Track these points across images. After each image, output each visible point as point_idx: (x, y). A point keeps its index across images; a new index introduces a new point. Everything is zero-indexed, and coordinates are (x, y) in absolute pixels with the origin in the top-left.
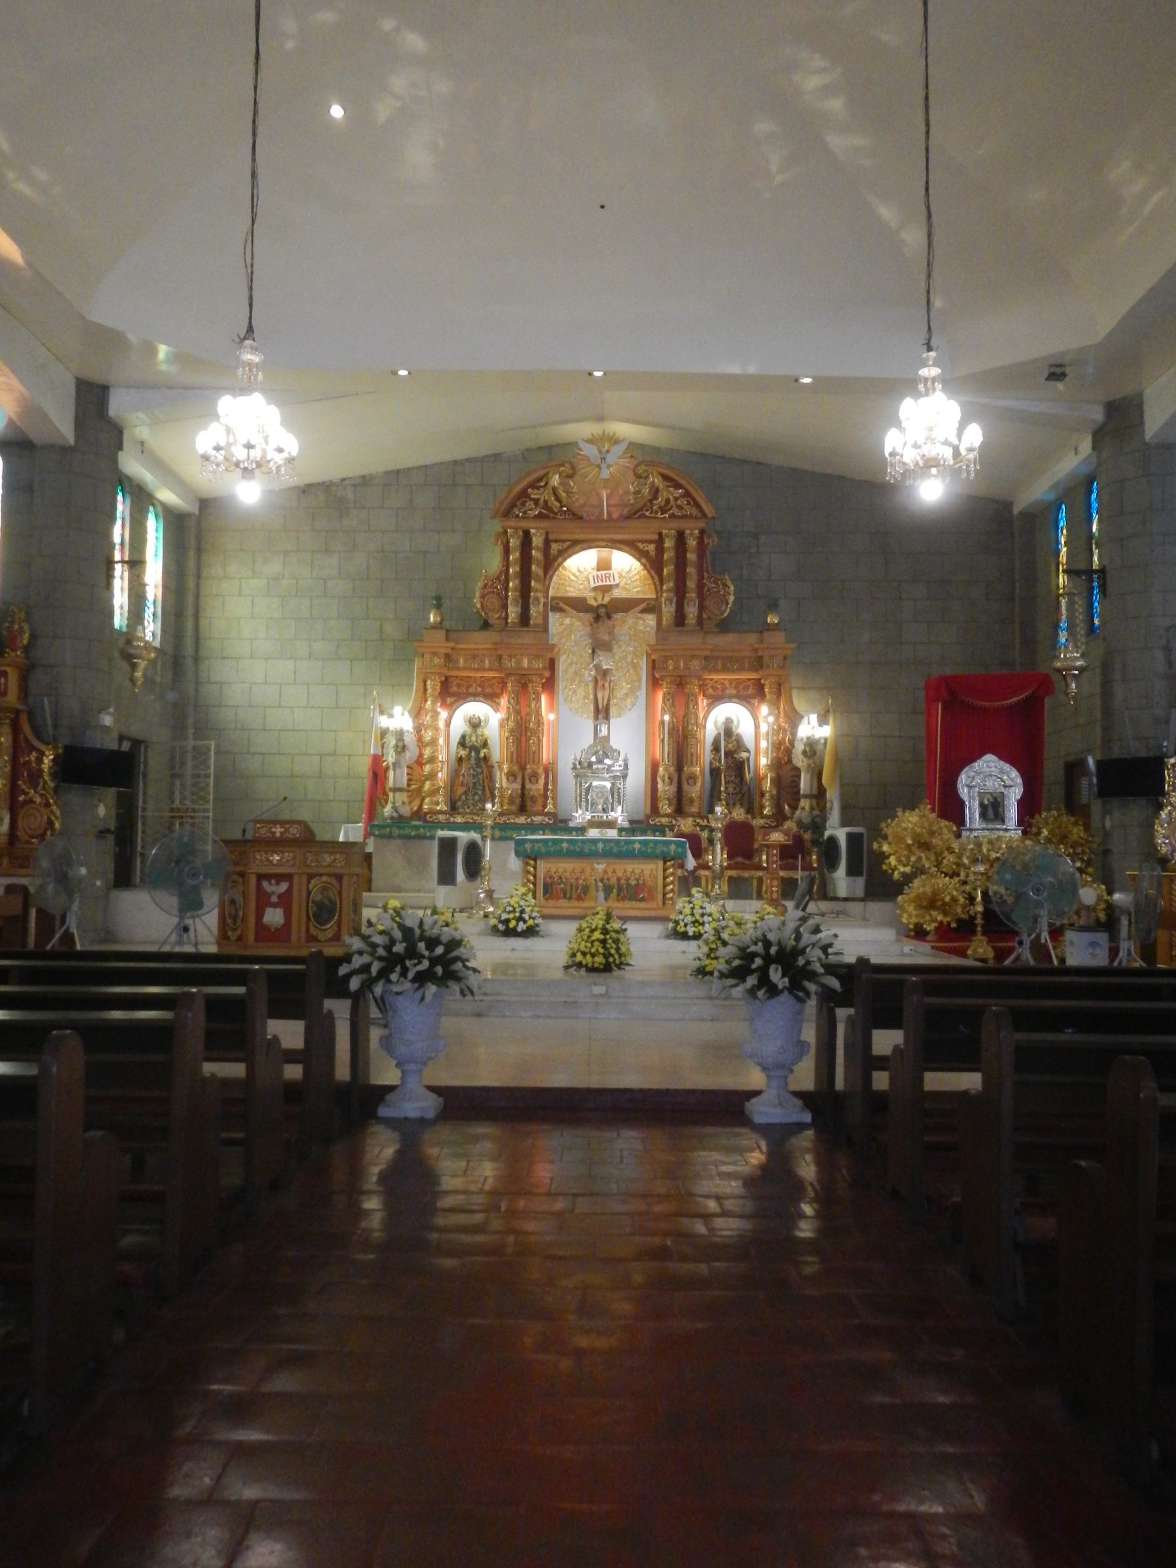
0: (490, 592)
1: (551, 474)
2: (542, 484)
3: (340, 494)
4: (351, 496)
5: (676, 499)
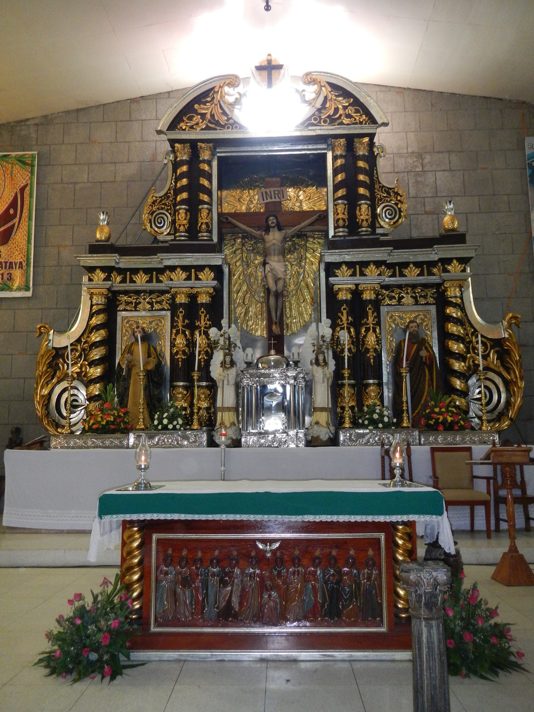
0: (158, 209)
1: (216, 90)
2: (209, 99)
3: (23, 133)
4: (34, 135)
5: (345, 108)
